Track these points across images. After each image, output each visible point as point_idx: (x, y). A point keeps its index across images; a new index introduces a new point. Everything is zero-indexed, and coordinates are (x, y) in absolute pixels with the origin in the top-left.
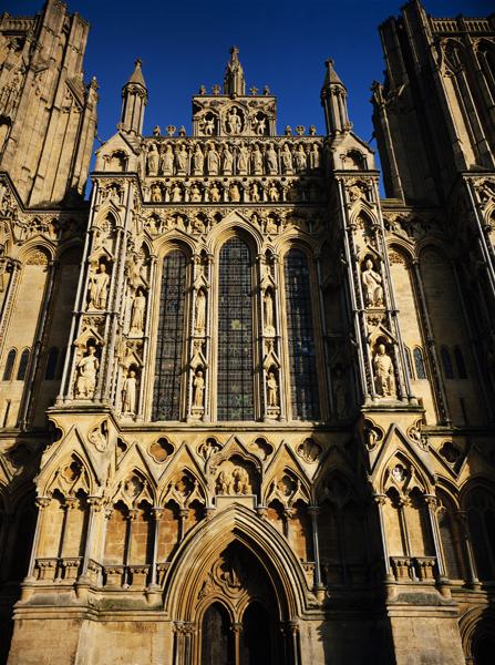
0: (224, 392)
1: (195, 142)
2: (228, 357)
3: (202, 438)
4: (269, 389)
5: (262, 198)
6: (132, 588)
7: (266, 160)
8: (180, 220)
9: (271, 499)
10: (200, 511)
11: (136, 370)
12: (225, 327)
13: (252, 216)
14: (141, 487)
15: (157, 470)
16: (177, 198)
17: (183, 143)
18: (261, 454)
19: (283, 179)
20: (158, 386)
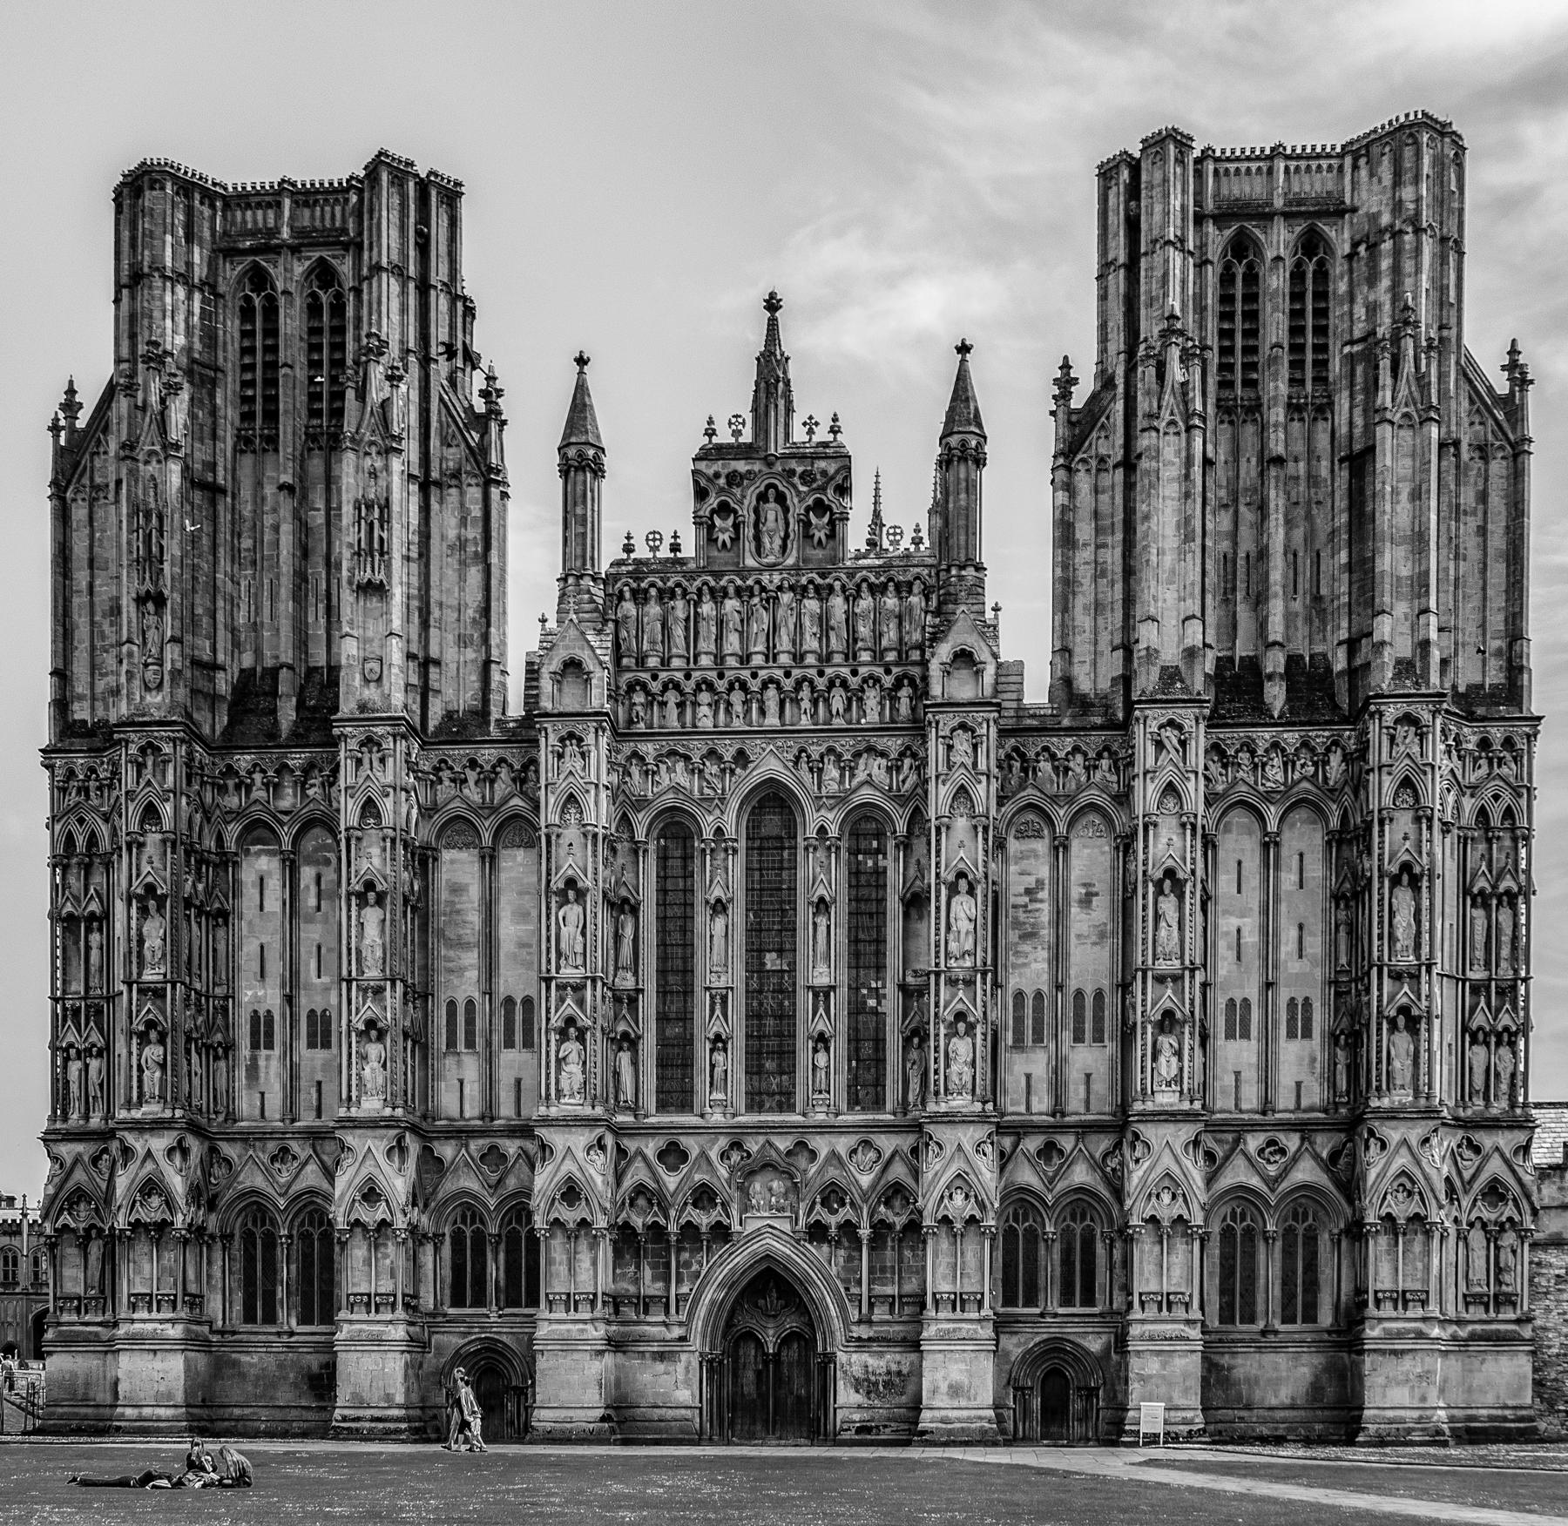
0: (754, 1069)
1: (698, 583)
2: (759, 1017)
3: (723, 1142)
4: (815, 1067)
5: (814, 715)
6: (649, 1319)
7: (824, 621)
8: (680, 766)
9: (812, 1220)
10: (721, 1233)
11: (630, 1042)
12: (755, 967)
13: (798, 758)
14: (651, 1205)
15: (671, 1181)
16: (672, 712)
17: (678, 585)
18: (802, 1161)
19: (854, 673)
20: (662, 1063)
